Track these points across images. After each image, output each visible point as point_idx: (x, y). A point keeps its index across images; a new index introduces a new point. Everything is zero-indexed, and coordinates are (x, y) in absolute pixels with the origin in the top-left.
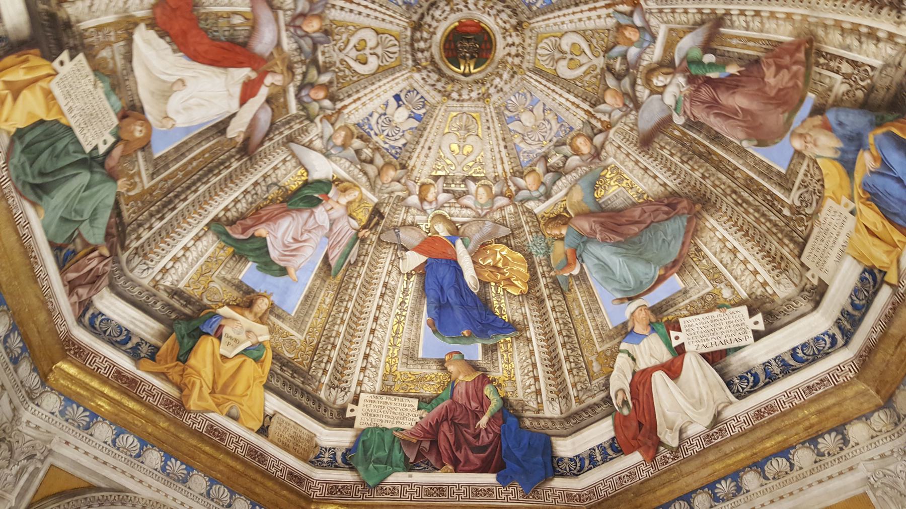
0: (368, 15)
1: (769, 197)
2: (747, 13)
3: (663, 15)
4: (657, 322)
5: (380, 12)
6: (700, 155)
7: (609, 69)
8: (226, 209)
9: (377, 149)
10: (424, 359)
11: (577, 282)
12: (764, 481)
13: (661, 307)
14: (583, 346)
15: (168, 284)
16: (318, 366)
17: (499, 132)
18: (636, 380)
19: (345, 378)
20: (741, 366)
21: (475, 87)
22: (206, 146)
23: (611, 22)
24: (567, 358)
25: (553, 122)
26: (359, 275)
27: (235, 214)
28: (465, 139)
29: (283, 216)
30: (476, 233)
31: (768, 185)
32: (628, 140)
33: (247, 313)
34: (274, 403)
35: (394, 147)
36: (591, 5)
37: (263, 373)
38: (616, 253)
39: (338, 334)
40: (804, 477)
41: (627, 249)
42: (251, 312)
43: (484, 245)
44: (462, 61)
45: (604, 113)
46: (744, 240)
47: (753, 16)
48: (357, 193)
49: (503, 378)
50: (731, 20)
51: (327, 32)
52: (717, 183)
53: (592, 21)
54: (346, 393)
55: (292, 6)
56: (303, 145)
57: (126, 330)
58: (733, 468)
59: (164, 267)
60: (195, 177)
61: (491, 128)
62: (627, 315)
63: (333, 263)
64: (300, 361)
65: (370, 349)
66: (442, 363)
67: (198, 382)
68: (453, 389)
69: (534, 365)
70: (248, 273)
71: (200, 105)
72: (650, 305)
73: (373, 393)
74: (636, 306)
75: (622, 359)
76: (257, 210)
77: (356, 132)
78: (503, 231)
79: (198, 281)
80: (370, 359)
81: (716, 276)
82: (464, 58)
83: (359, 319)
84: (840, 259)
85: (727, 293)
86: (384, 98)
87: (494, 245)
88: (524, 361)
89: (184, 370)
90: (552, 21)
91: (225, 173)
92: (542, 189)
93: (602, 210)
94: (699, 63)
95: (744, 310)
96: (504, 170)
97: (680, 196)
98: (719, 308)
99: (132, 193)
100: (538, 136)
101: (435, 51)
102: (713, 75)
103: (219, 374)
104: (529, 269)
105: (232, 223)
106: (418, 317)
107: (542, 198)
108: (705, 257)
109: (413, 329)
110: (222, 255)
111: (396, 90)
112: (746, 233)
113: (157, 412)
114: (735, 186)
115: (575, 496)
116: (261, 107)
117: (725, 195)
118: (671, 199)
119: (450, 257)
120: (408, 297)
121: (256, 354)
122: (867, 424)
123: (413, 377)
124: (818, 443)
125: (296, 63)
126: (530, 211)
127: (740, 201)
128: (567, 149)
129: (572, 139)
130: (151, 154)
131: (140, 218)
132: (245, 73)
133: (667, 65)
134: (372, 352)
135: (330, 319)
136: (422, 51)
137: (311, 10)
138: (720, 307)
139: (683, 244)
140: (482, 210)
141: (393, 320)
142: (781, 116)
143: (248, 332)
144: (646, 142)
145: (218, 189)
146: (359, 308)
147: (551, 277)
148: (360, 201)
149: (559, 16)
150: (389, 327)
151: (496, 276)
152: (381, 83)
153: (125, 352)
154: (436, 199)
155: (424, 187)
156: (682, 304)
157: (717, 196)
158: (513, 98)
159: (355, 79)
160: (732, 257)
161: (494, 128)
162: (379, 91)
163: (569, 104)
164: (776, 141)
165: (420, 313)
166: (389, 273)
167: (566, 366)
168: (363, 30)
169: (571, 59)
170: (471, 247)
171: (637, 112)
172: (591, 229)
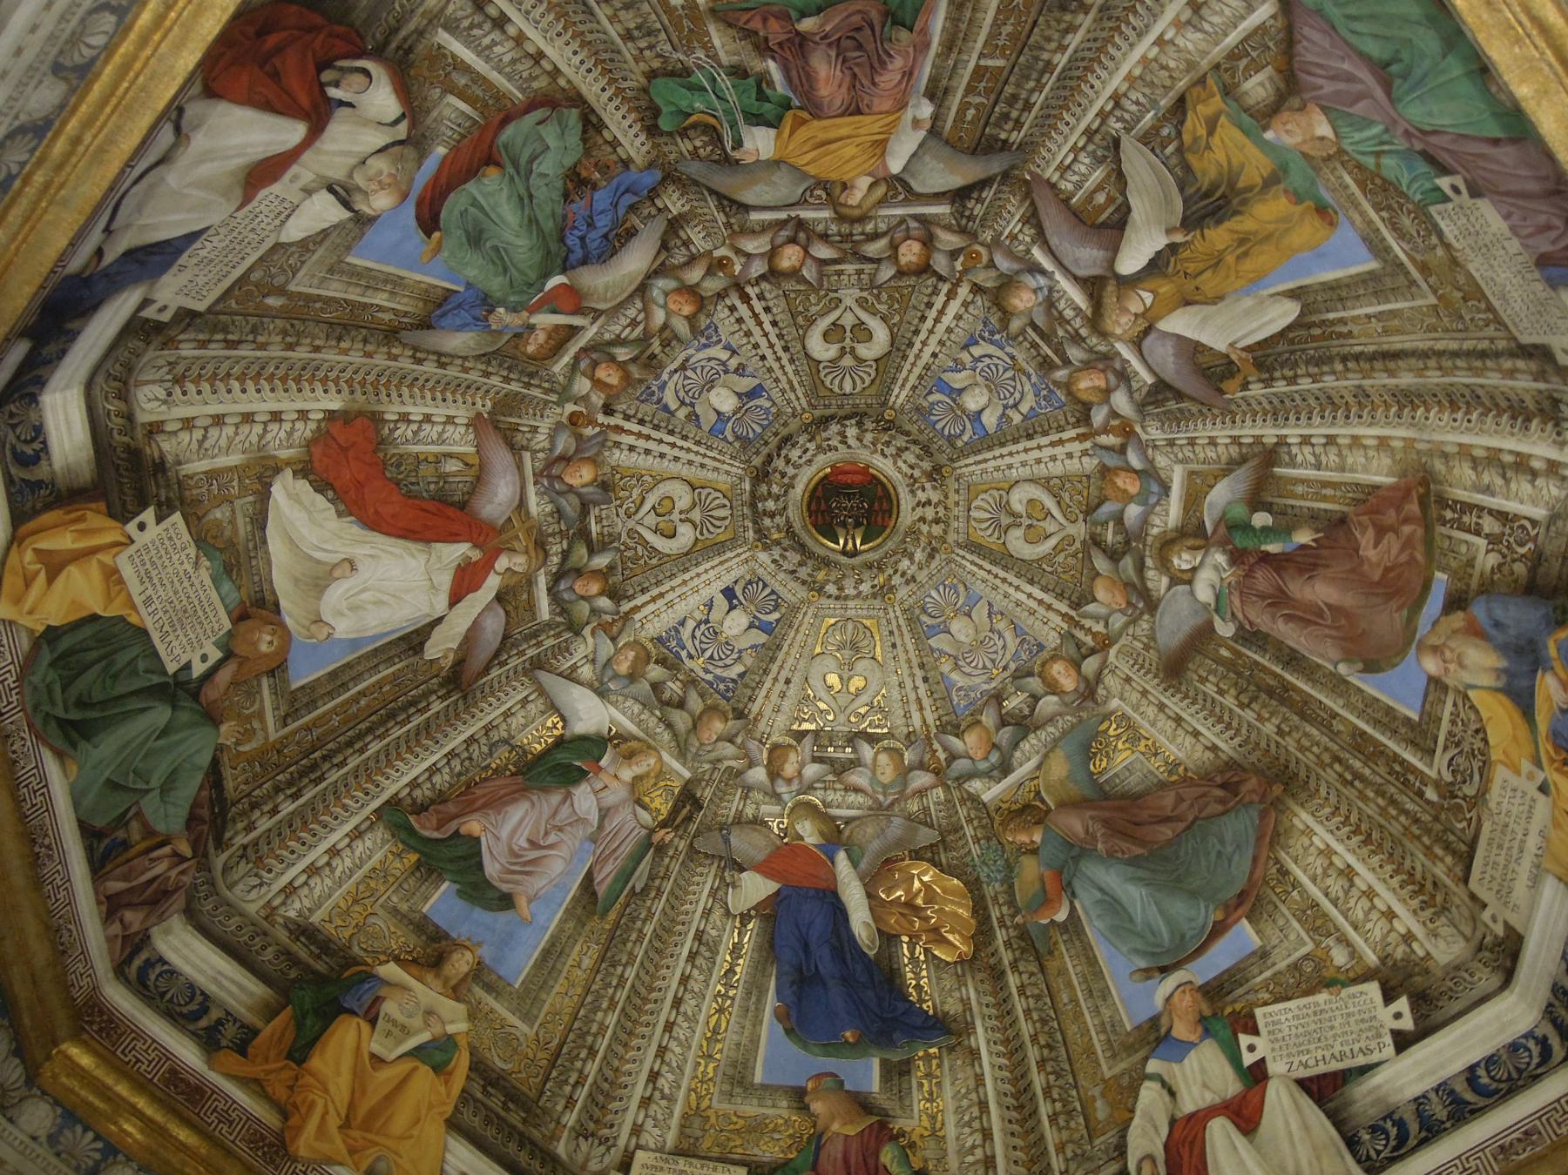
0: (676, 459)
2: (1314, 440)
3: (1176, 449)
4: (1214, 1015)
5: (697, 453)
6: (1271, 693)
7: (1096, 541)
8: (414, 784)
9: (692, 682)
10: (764, 1087)
11: (1065, 937)
13: (1221, 986)
14: (1077, 1066)
15: (292, 914)
16: (556, 1090)
17: (912, 655)
18: (1176, 1135)
19: (609, 1117)
20: (1373, 1106)
21: (866, 575)
22: (386, 672)
23: (1090, 464)
24: (1047, 1091)
25: (1008, 635)
26: (650, 915)
27: (428, 793)
29: (515, 800)
30: (872, 839)
31: (1393, 745)
32: (1142, 667)
33: (430, 977)
35: (723, 680)
36: (1055, 437)
37: (448, 1095)
39: (603, 1028)
41: (1153, 871)
42: (437, 976)
43: (888, 861)
44: (841, 532)
45: (1096, 618)
46: (1365, 851)
47: (1325, 445)
48: (652, 761)
49: (919, 1131)
50: (1289, 453)
51: (605, 486)
52: (1307, 743)
53: (1058, 463)
54: (608, 1149)
55: (546, 444)
57: (203, 993)
59: (291, 883)
60: (363, 726)
61: (899, 643)
63: (601, 890)
64: (526, 1081)
65: (663, 1062)
66: (799, 1097)
67: (320, 1103)
68: (818, 1149)
69: (983, 1105)
72: (1200, 981)
73: (660, 1150)
74: (1175, 984)
75: (1149, 1094)
76: (469, 787)
77: (654, 651)
78: (926, 836)
79: (347, 912)
80: (661, 1082)
81: (1319, 922)
82: (844, 525)
83: (645, 1000)
84: (1535, 882)
85: (1339, 957)
86: (706, 593)
87: (907, 862)
88: (964, 1097)
89: (297, 1079)
90: (992, 464)
91: (417, 720)
92: (995, 757)
93: (1106, 796)
94: (1246, 527)
95: (1373, 990)
97: (1244, 770)
98: (1328, 986)
99: (241, 749)
100: (982, 659)
101: (795, 515)
102: (1273, 548)
103: (364, 1092)
104: (975, 912)
105: (420, 809)
106: (759, 1000)
107: (995, 773)
108: (1296, 884)
109: (748, 1024)
110: (397, 866)
111: (727, 580)
112: (1368, 837)
113: (229, 1153)
114: (1336, 747)
116: (488, 608)
117: (1322, 765)
118: (1228, 775)
119: (822, 885)
120: (741, 961)
121: (438, 1057)
123: (741, 1122)
125: (553, 535)
126: (974, 799)
127: (1349, 777)
128: (1034, 683)
129: (1043, 665)
130: (286, 681)
132: (459, 551)
133: (1192, 533)
134: (665, 1068)
135: (589, 999)
136: (772, 515)
137: (577, 451)
138: (1329, 984)
139: (1255, 859)
140: (885, 795)
141: (709, 1006)
142: (1396, 615)
143: (429, 1013)
144: (1174, 669)
145: (403, 748)
146: (647, 979)
148: (657, 777)
149: (1002, 456)
150: (702, 1018)
151: (912, 923)
152: (701, 569)
153: (194, 1035)
154: (800, 773)
155: (778, 752)
156: (1259, 979)
158: (934, 593)
159: (654, 561)
160: (1347, 885)
161: (904, 645)
162: (696, 581)
163: (1033, 604)
164: (1395, 661)
165: (762, 992)
166: (707, 913)
167: (1044, 1109)
168: (668, 483)
169: (1030, 526)
171: (1153, 616)
172: (1087, 832)
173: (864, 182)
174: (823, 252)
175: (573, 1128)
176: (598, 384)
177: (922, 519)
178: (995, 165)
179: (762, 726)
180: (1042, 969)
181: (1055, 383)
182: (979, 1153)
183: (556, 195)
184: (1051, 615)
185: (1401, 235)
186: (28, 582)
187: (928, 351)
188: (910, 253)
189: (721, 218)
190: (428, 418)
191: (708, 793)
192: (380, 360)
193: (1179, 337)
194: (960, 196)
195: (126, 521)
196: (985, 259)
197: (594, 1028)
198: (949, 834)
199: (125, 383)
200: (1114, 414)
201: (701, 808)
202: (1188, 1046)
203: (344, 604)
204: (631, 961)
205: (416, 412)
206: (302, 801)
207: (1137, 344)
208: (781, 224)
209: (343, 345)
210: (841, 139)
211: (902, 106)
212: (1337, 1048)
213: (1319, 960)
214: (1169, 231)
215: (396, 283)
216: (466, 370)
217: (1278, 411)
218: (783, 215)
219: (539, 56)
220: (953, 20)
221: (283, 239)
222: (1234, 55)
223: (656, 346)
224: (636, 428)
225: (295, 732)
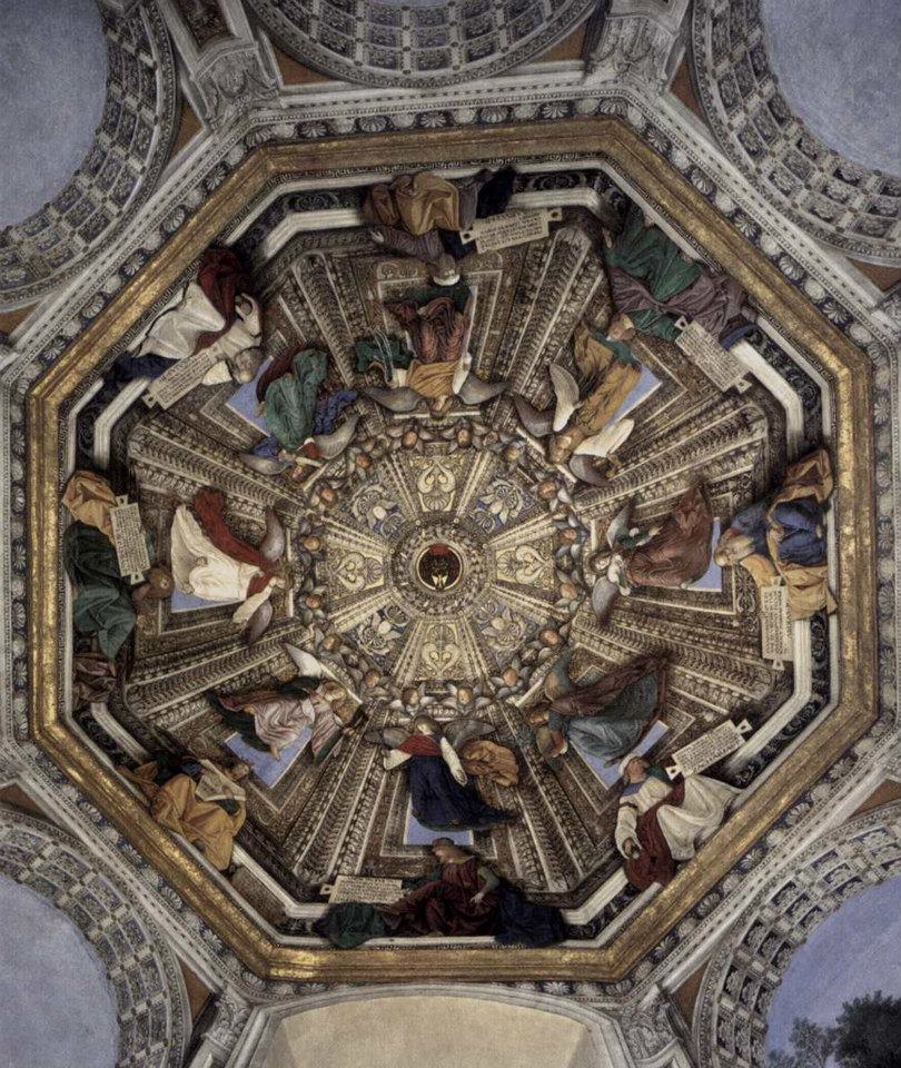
1: (718, 621)
6: (652, 615)
7: (558, 567)
8: (222, 685)
9: (362, 656)
15: (159, 725)
23: (552, 530)
25: (521, 624)
28: (443, 649)
29: (272, 702)
34: (241, 856)
35: (378, 656)
38: (599, 723)
42: (231, 772)
45: (564, 606)
56: (297, 647)
60: (202, 647)
62: (621, 771)
63: (316, 753)
68: (442, 871)
70: (233, 740)
71: (215, 584)
72: (641, 755)
78: (487, 729)
83: (339, 811)
85: (709, 718)
86: (370, 612)
91: (226, 654)
92: (520, 684)
93: (577, 687)
96: (482, 672)
102: (641, 543)
104: (517, 762)
105: (225, 696)
108: (681, 697)
111: (381, 606)
119: (433, 753)
121: (230, 808)
126: (512, 707)
128: (536, 644)
131: (148, 660)
132: (253, 570)
133: (604, 550)
135: (309, 804)
137: (311, 533)
139: (659, 693)
140: (464, 709)
144: (605, 621)
147: (540, 763)
154: (419, 702)
157: (677, 645)
165: (404, 807)
170: (455, 744)
173: (443, 398)
174: (426, 436)
175: (301, 864)
176: (323, 500)
177: (475, 572)
178: (498, 389)
179: (399, 680)
180: (557, 779)
181: (533, 493)
182: (534, 869)
183: (313, 395)
184: (541, 610)
185: (667, 362)
186: (76, 496)
187: (473, 487)
188: (463, 436)
189: (381, 419)
190: (246, 502)
191: (371, 712)
192: (228, 467)
193: (585, 456)
194: (483, 406)
195: (116, 495)
196: (496, 438)
197: (312, 819)
198: (499, 728)
199: (126, 435)
200: (560, 503)
201: (367, 719)
202: (639, 785)
203: (200, 580)
204: (331, 791)
205: (242, 498)
206: (167, 676)
207: (567, 463)
208: (407, 421)
209: (216, 454)
210: (433, 375)
211: (458, 357)
212: (716, 752)
213: (700, 721)
214: (574, 404)
215: (242, 425)
216: (265, 482)
217: (634, 479)
218: (407, 417)
219: (314, 323)
220: (479, 308)
221: (204, 382)
222: (589, 308)
223: (350, 483)
224: (338, 525)
225: (170, 636)
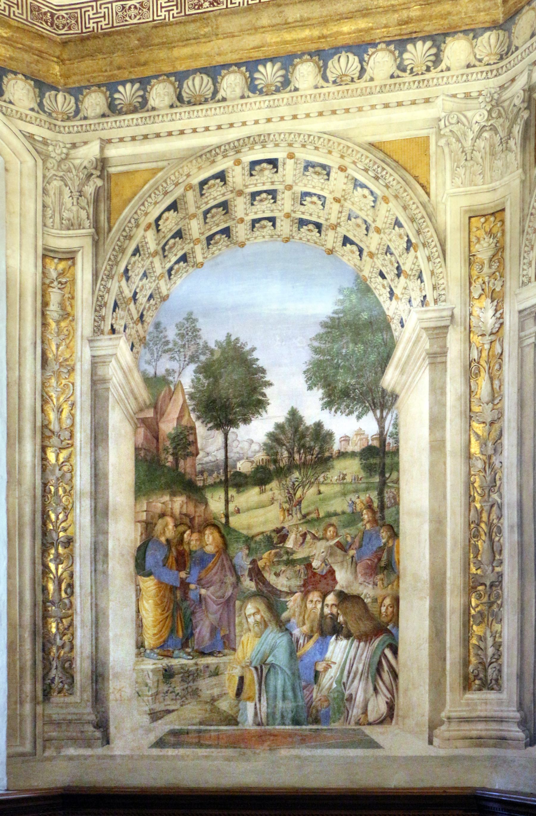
12: (322, 83)
40: (371, 93)
58: (290, 48)
115: (45, 13)
122: (472, 44)
124: (405, 50)
